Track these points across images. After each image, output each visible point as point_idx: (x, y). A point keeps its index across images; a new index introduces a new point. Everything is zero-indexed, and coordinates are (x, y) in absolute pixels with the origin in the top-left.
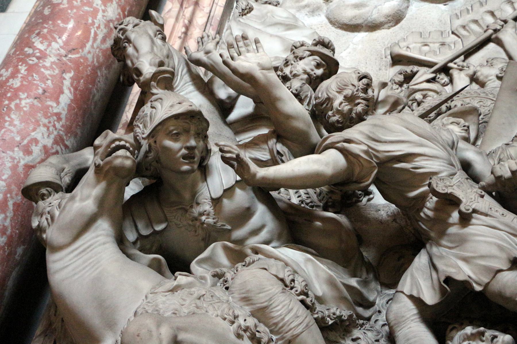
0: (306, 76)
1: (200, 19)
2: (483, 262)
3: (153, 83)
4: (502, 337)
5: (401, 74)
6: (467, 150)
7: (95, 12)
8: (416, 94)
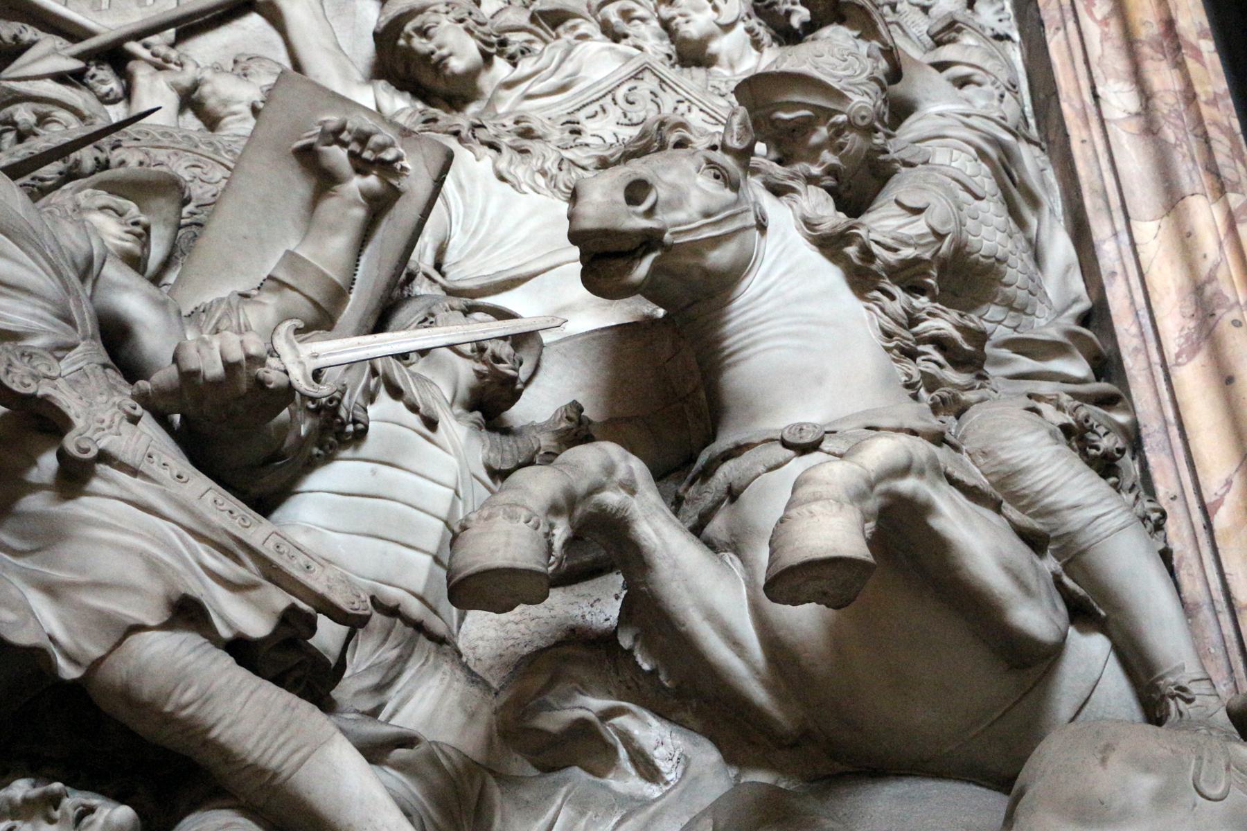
2: (96, 601)
4: (106, 812)
6: (126, 288)
8: (18, 106)
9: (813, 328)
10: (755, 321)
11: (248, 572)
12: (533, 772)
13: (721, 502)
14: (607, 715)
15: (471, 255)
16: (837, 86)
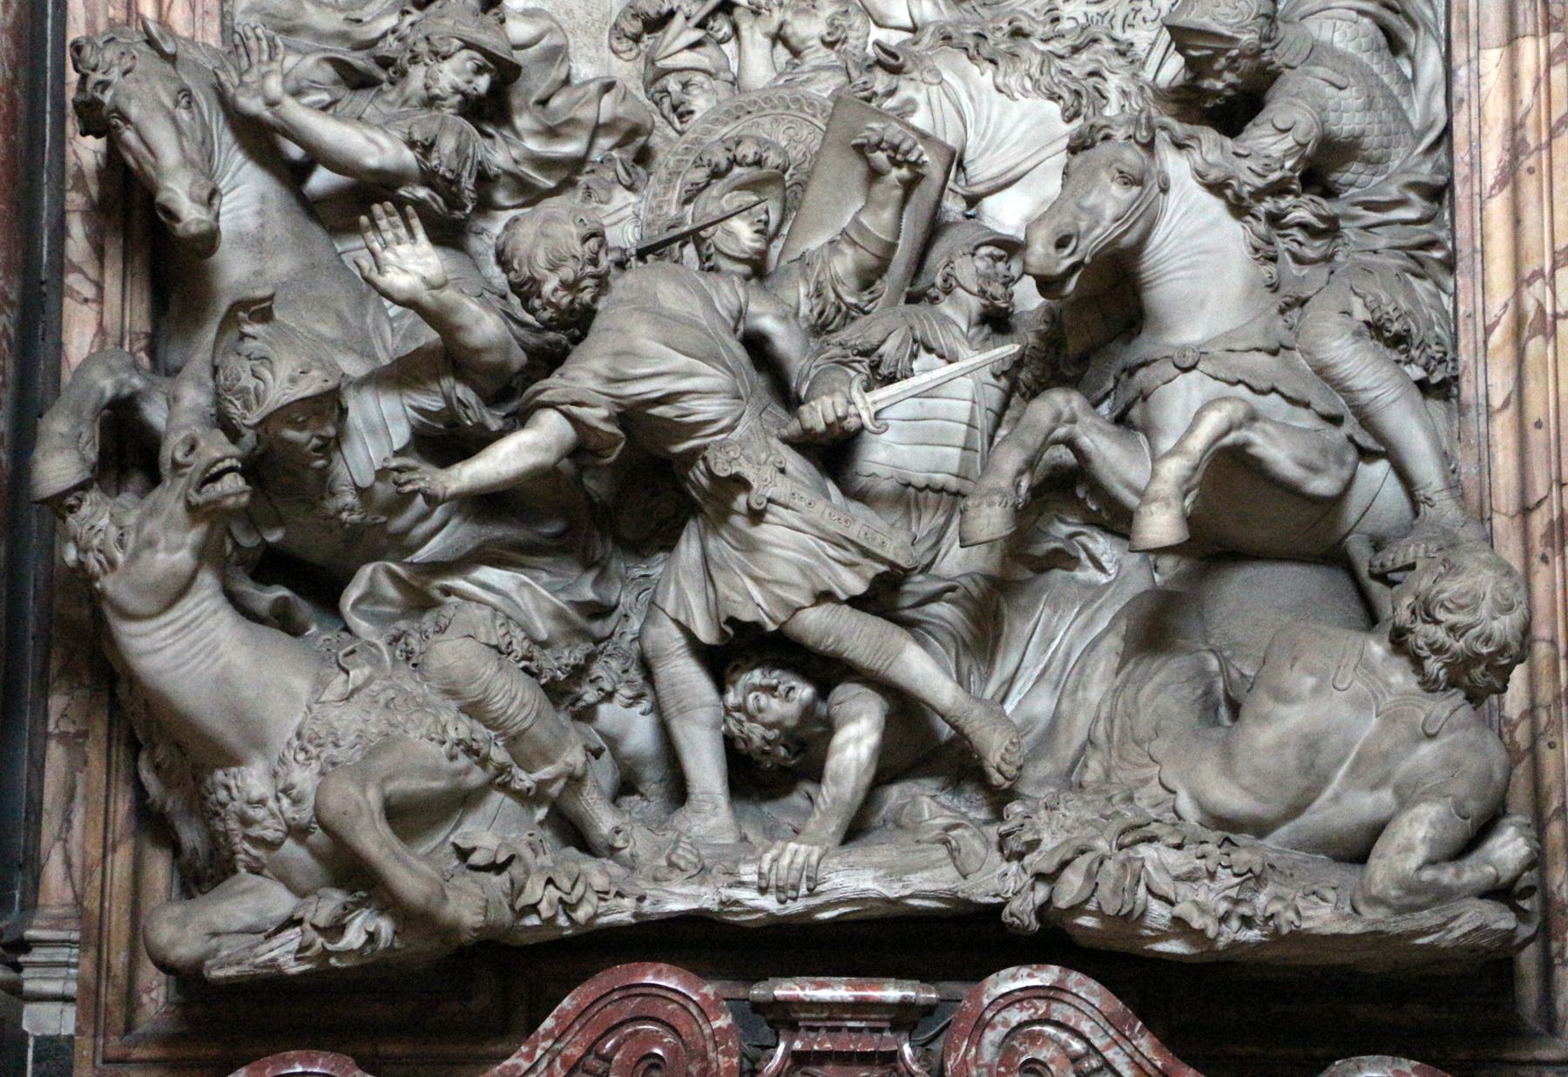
0: (458, 98)
2: (779, 591)
3: (241, 314)
5: (635, 16)
9: (1202, 257)
10: (1160, 262)
12: (1029, 574)
13: (1135, 399)
14: (1072, 536)
15: (981, 155)
16: (1228, 33)
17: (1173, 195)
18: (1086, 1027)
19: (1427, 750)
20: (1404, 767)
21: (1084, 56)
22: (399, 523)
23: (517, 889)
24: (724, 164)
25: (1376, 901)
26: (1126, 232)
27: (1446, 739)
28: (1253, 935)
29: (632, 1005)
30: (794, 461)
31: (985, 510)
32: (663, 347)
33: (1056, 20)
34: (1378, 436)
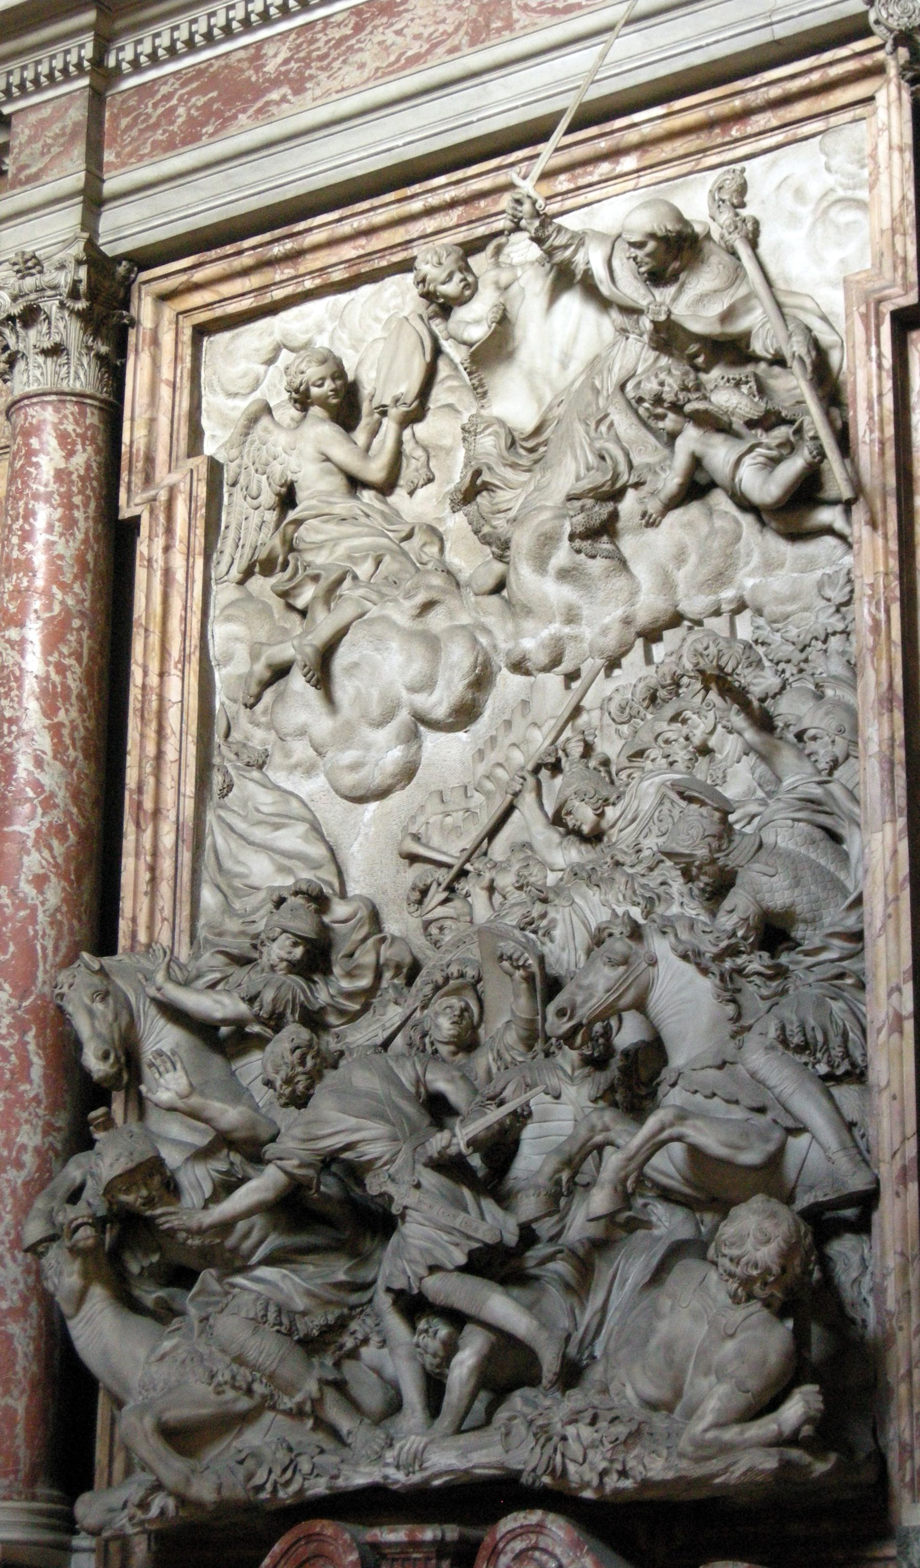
0: (284, 964)
1: (167, 840)
7: (34, 909)
11: (456, 1239)
17: (661, 965)
18: (558, 1551)
19: (730, 1346)
20: (716, 1359)
21: (656, 872)
22: (231, 1242)
23: (250, 1477)
24: (440, 981)
25: (681, 1455)
26: (619, 997)
27: (741, 1336)
28: (628, 1483)
29: (313, 1546)
30: (430, 1178)
31: (525, 1201)
32: (341, 1115)
33: (639, 851)
34: (795, 1118)
